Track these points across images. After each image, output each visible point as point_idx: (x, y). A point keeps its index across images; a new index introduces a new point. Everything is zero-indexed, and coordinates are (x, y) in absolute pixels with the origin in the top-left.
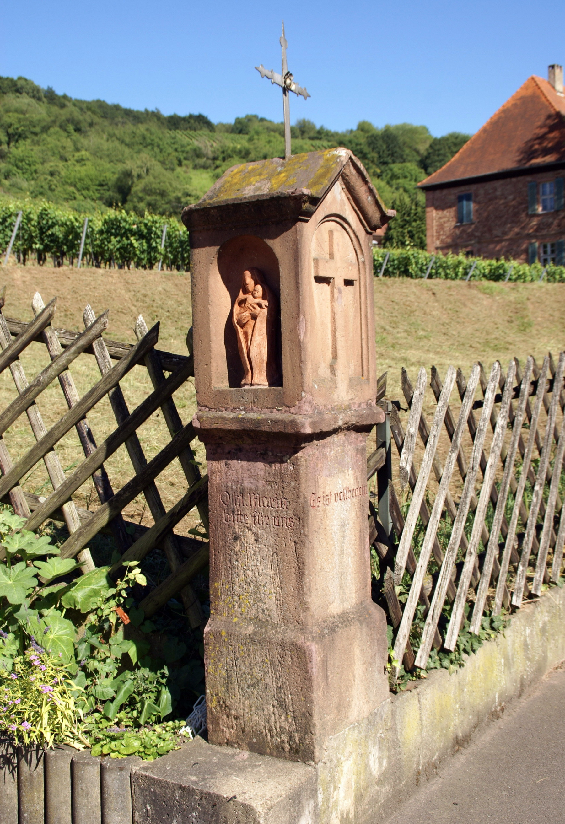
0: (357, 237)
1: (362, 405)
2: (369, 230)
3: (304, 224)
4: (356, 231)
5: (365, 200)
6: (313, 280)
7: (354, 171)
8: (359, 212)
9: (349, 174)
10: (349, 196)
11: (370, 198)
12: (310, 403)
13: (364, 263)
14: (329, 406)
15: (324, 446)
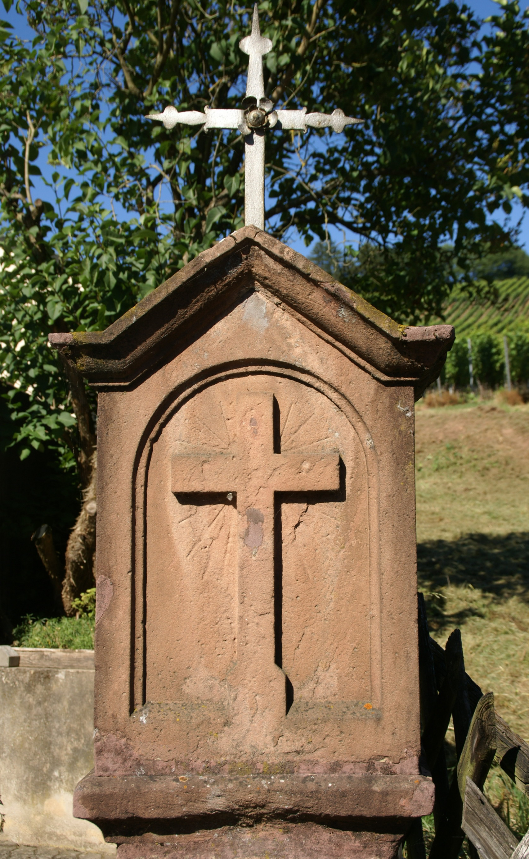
0: (343, 396)
1: (347, 768)
2: (385, 378)
3: (117, 395)
4: (336, 385)
5: (333, 318)
6: (172, 501)
7: (278, 267)
8: (337, 344)
9: (267, 274)
10: (299, 316)
11: (343, 312)
12: (118, 752)
13: (373, 448)
14: (199, 764)
15: (196, 847)
